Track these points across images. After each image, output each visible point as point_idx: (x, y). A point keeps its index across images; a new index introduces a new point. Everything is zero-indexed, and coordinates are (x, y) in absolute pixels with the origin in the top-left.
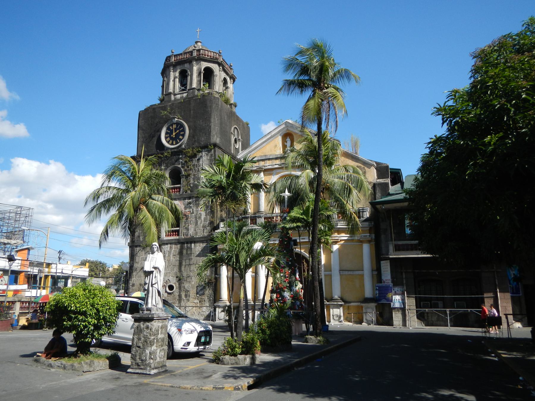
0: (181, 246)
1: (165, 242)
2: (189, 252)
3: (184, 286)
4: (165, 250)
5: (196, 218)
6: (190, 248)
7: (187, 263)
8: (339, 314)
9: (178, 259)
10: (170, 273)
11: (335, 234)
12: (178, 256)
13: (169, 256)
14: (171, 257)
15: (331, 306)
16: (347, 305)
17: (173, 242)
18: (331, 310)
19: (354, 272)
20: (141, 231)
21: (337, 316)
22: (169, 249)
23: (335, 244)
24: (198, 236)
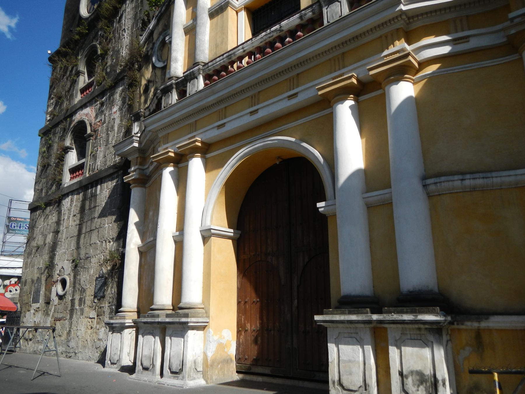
0: (83, 195)
1: (65, 192)
2: (92, 206)
3: (80, 280)
4: (65, 208)
5: (107, 130)
6: (94, 196)
7: (88, 230)
8: (428, 371)
9: (78, 222)
10: (65, 253)
11: (397, 43)
12: (78, 216)
13: (69, 218)
14: (71, 220)
15: (393, 333)
16: (472, 325)
17: (74, 188)
18: (393, 352)
19: (494, 174)
20: (45, 179)
21: (421, 378)
22: (69, 203)
23: (397, 81)
24: (107, 167)
